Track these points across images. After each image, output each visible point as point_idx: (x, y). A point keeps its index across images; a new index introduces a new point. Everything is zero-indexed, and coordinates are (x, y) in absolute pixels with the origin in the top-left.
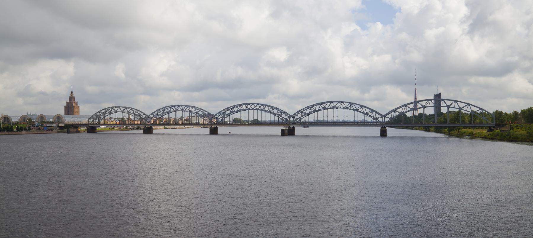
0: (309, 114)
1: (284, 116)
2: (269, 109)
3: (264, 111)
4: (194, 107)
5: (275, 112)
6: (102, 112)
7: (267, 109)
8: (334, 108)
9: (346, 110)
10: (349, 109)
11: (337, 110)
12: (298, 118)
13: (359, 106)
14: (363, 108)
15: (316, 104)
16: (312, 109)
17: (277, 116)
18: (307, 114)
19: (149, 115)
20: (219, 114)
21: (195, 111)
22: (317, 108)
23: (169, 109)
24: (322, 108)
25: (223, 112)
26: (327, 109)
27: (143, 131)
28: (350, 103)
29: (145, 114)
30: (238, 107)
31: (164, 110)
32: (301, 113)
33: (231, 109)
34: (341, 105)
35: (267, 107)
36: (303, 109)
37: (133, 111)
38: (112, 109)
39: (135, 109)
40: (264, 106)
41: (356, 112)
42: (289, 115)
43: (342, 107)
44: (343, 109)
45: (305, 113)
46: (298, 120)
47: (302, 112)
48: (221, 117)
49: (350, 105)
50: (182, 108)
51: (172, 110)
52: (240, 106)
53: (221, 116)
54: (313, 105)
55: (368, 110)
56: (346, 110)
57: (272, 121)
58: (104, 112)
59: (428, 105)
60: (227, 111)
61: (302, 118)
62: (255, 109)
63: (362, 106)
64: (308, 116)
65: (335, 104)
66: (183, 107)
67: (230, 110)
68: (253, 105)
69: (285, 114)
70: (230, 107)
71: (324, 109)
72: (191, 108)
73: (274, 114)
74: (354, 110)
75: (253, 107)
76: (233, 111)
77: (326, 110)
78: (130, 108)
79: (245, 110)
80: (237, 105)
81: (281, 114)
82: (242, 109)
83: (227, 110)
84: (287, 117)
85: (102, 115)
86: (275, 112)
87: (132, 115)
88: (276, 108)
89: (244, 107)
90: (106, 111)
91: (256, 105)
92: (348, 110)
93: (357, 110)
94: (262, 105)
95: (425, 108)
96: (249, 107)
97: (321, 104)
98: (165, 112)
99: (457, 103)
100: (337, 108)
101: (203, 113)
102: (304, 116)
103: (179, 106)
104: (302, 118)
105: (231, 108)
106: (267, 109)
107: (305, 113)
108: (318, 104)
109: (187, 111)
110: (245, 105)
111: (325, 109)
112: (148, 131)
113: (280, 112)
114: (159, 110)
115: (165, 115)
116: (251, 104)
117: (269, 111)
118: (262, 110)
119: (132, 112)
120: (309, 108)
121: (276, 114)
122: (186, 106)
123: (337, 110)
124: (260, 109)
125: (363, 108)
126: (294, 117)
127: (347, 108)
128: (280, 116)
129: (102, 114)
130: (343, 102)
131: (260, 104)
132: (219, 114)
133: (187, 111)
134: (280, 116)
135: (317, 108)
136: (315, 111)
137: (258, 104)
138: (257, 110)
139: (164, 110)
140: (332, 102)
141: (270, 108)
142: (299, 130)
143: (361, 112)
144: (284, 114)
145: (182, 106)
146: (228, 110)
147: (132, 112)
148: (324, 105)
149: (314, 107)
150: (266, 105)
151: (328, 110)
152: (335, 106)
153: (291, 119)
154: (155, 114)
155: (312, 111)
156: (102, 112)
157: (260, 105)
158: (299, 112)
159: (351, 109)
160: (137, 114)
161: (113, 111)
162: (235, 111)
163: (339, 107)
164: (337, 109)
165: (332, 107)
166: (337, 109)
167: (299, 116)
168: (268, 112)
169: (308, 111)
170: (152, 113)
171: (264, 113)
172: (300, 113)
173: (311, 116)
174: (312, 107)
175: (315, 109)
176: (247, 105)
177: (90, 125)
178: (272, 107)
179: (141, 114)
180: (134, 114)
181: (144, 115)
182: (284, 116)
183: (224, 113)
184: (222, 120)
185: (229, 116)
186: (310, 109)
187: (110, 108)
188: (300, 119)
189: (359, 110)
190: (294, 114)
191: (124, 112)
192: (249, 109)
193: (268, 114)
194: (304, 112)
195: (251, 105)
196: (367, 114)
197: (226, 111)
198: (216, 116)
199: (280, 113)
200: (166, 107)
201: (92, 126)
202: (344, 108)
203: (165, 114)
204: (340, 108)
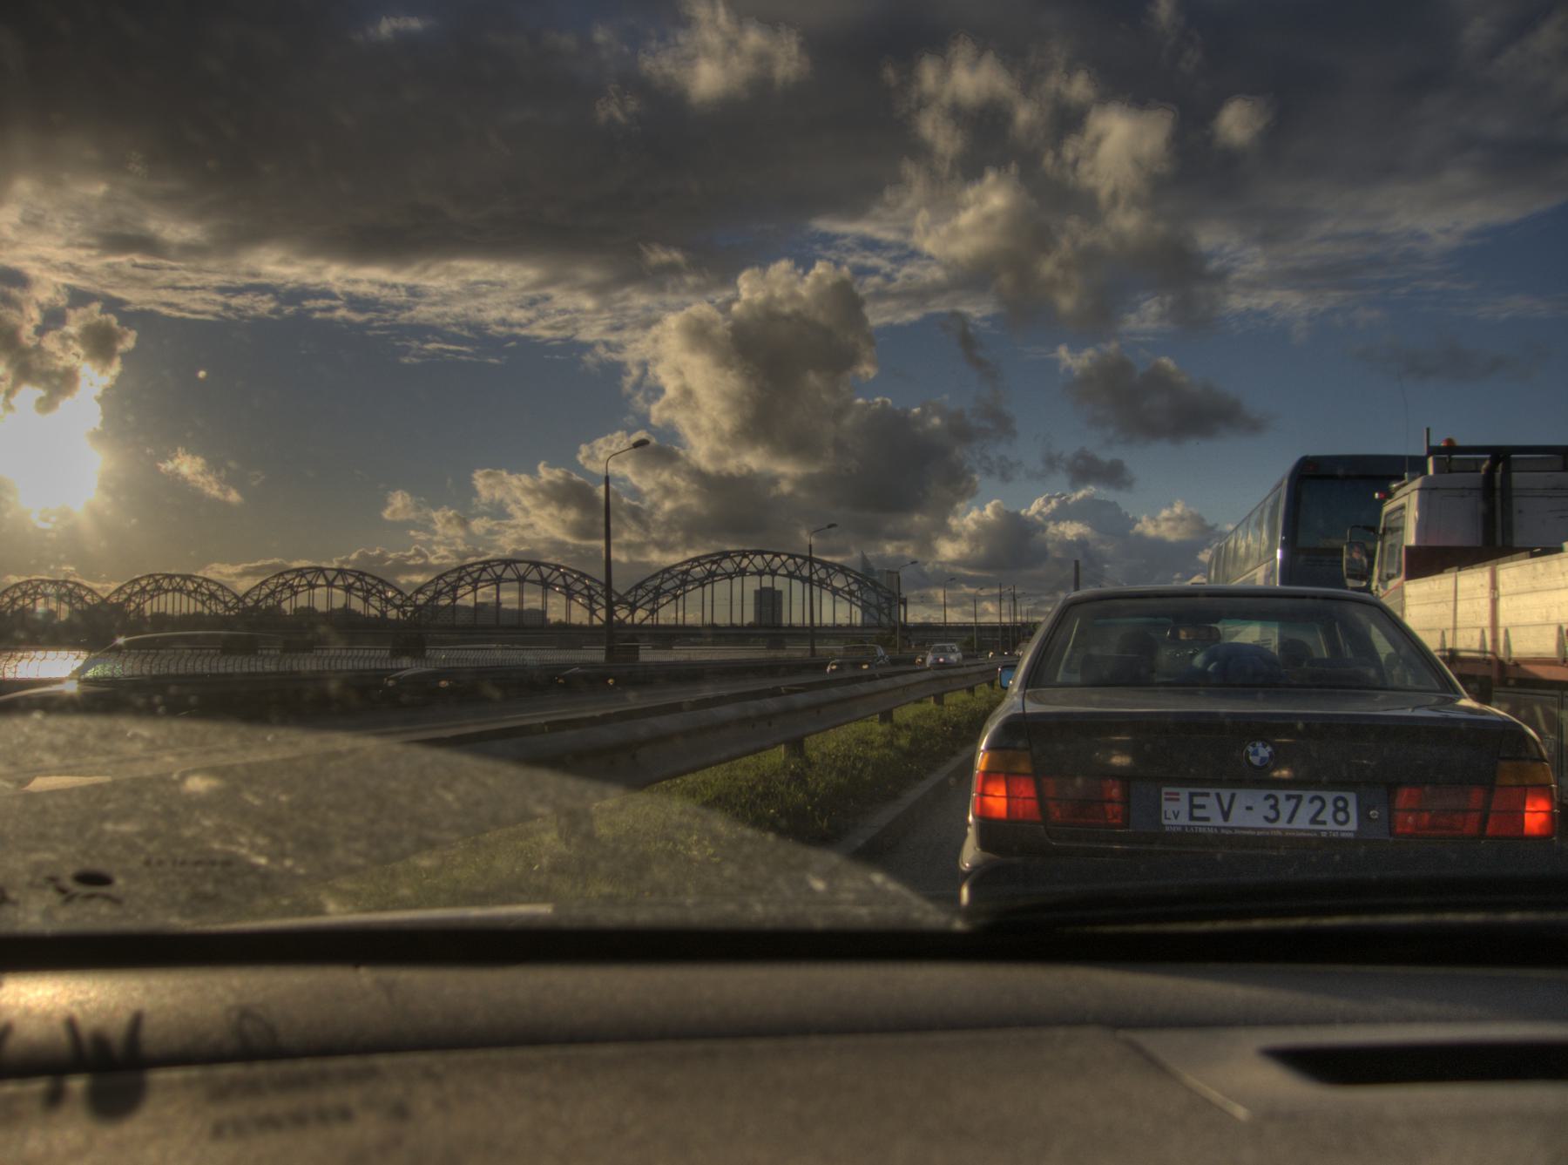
3: (797, 578)
31: (461, 579)
38: (484, 570)
40: (799, 561)
58: (452, 579)
75: (758, 561)
78: (356, 572)
87: (358, 596)
91: (768, 557)
96: (745, 562)
110: (731, 558)
121: (842, 589)
129: (447, 589)
156: (446, 582)
157: (784, 558)
161: (485, 576)
181: (399, 596)
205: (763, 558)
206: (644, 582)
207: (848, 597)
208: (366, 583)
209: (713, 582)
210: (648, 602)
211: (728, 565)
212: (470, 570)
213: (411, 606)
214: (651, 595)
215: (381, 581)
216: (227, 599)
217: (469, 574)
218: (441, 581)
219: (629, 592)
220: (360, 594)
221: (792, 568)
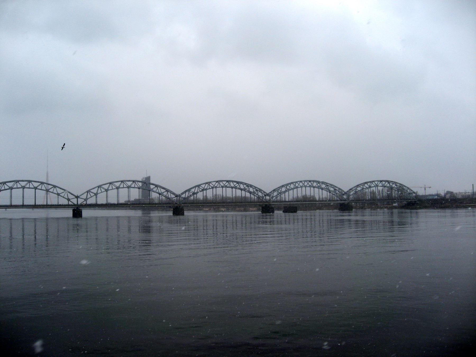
9: (224, 189)
20: (351, 191)
37: (389, 183)
50: (376, 184)
57: (325, 198)
59: (15, 186)
66: (376, 183)
73: (250, 193)
95: (12, 189)
99: (6, 185)
118: (310, 186)
128: (256, 194)
138: (306, 187)
142: (86, 213)
144: (261, 192)
153: (268, 198)
158: (274, 190)
206: (352, 188)
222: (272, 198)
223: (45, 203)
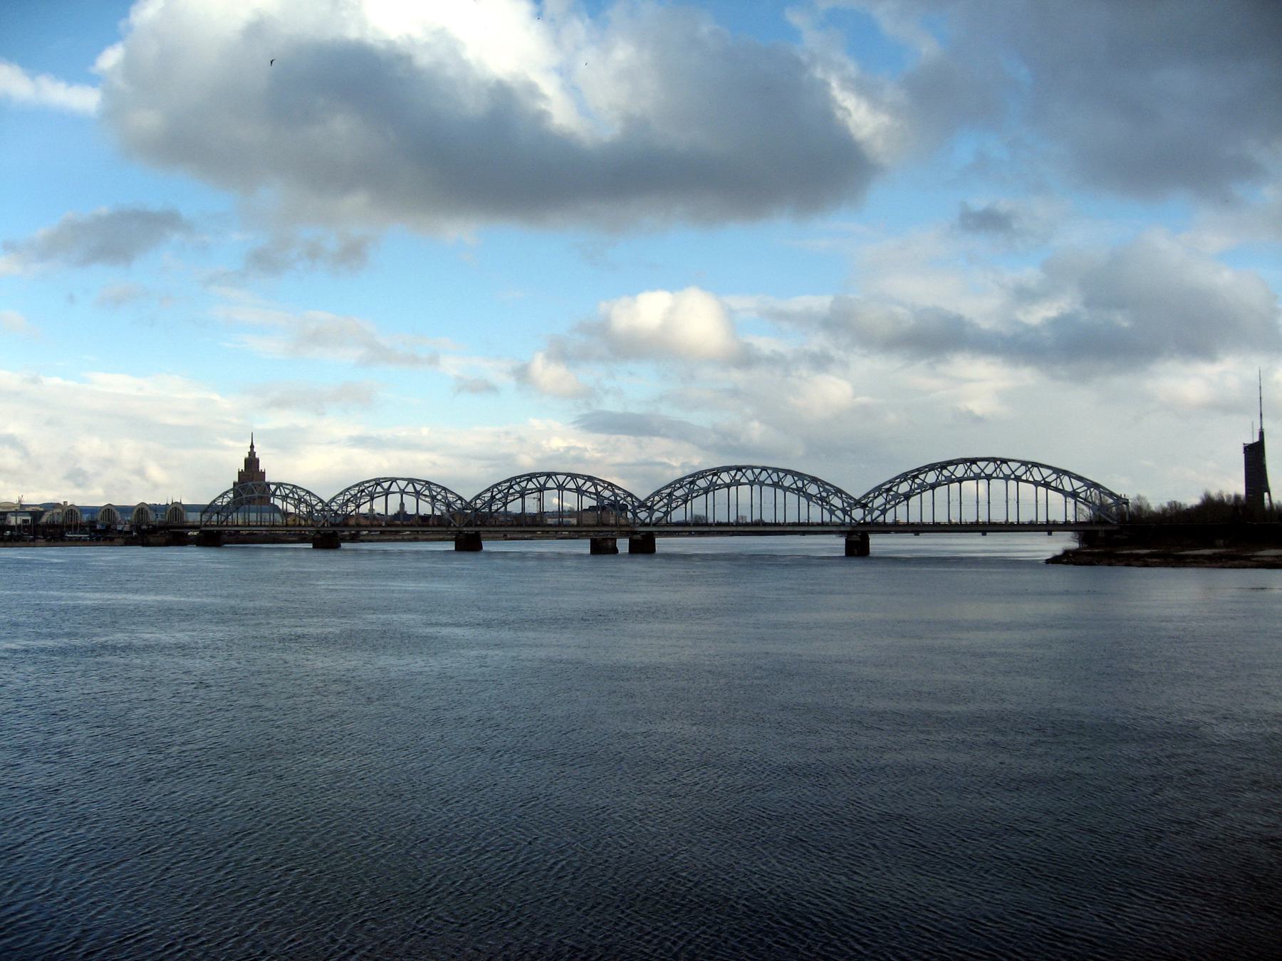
0: (907, 497)
1: (836, 501)
2: (795, 482)
4: (590, 479)
5: (813, 490)
6: (352, 492)
7: (788, 481)
8: (977, 477)
10: (1024, 481)
11: (989, 484)
12: (875, 507)
13: (1051, 472)
14: (1061, 480)
15: (926, 467)
16: (917, 481)
17: (818, 503)
18: (903, 494)
19: (471, 502)
21: (592, 490)
22: (931, 477)
23: (523, 484)
24: (943, 478)
25: (668, 491)
26: (960, 480)
27: (454, 542)
28: (1024, 463)
29: (460, 498)
30: (710, 478)
31: (511, 487)
32: (885, 495)
33: (692, 483)
34: (998, 470)
35: (789, 477)
36: (890, 482)
39: (435, 485)
40: (781, 475)
41: (1042, 490)
42: (851, 498)
43: (1001, 475)
44: (1003, 481)
45: (896, 492)
46: (877, 513)
47: (889, 490)
48: (663, 507)
49: (1023, 468)
51: (531, 485)
52: (714, 474)
53: (661, 504)
54: (920, 470)
55: (1077, 484)
56: (1012, 484)
60: (679, 488)
61: (888, 506)
62: (756, 484)
63: (1059, 472)
64: (905, 502)
65: (982, 464)
67: (688, 486)
68: (750, 471)
69: (841, 498)
70: (685, 478)
71: (950, 481)
72: (580, 482)
74: (1036, 484)
76: (696, 488)
77: (958, 484)
79: (728, 486)
80: (706, 471)
81: (828, 496)
82: (719, 482)
83: (678, 485)
84: (845, 505)
85: (352, 501)
86: (813, 490)
87: (427, 502)
88: (814, 480)
89: (726, 478)
90: (363, 491)
92: (1020, 483)
93: (1047, 485)
94: (776, 470)
97: (944, 466)
98: (511, 491)
100: (989, 477)
101: (615, 495)
102: (893, 503)
103: (549, 475)
104: (888, 506)
105: (691, 479)
106: (788, 481)
107: (896, 492)
108: (932, 467)
109: (570, 490)
111: (953, 481)
112: (468, 544)
113: (825, 490)
114: (496, 486)
115: (514, 500)
116: (744, 467)
117: (794, 486)
119: (427, 493)
120: (905, 480)
121: (815, 496)
122: (568, 475)
123: (989, 484)
124: (769, 482)
125: (1061, 480)
126: (864, 506)
127: (1018, 479)
130: (1004, 461)
131: (770, 468)
132: (657, 498)
133: (570, 490)
134: (827, 503)
135: (931, 477)
136: (923, 487)
137: (764, 469)
139: (511, 487)
140: (974, 461)
141: (796, 478)
143: (1056, 489)
145: (555, 474)
146: (681, 487)
147: (427, 493)
148: (951, 468)
149: (922, 476)
150: (787, 472)
151: (964, 483)
152: (982, 471)
154: (486, 499)
155: (916, 486)
157: (770, 472)
159: (1027, 481)
160: (439, 497)
162: (701, 489)
163: (994, 475)
164: (989, 480)
165: (972, 475)
166: (989, 480)
167: (879, 501)
168: (793, 490)
169: (904, 488)
170: (478, 497)
171: (779, 492)
172: (881, 494)
173: (914, 501)
174: (916, 477)
175: (924, 481)
176: (733, 473)
177: (203, 529)
178: (801, 476)
179: (451, 498)
180: (433, 498)
181: (459, 502)
182: (836, 501)
183: (670, 495)
184: (666, 513)
185: (685, 502)
186: (910, 482)
187: (371, 481)
188: (884, 512)
189: (1052, 484)
190: (865, 496)
191: (407, 493)
192: (738, 483)
193: (791, 497)
194: (894, 489)
195: (744, 471)
196: (1074, 495)
197: (675, 490)
198: (649, 504)
199: (824, 494)
200: (515, 478)
201: (210, 531)
202: (1007, 478)
203: (512, 498)
204: (997, 478)
205: (753, 472)
207: (820, 502)
208: (298, 495)
209: (715, 490)
210: (663, 507)
211: (726, 478)
212: (518, 480)
213: (470, 509)
214: (665, 501)
215: (444, 489)
216: (314, 503)
217: (518, 483)
218: (495, 490)
219: (649, 498)
220: (292, 502)
221: (776, 479)
222: (872, 511)
223: (820, 521)
